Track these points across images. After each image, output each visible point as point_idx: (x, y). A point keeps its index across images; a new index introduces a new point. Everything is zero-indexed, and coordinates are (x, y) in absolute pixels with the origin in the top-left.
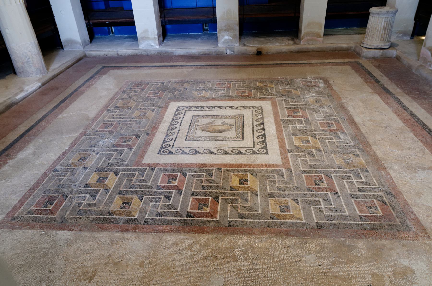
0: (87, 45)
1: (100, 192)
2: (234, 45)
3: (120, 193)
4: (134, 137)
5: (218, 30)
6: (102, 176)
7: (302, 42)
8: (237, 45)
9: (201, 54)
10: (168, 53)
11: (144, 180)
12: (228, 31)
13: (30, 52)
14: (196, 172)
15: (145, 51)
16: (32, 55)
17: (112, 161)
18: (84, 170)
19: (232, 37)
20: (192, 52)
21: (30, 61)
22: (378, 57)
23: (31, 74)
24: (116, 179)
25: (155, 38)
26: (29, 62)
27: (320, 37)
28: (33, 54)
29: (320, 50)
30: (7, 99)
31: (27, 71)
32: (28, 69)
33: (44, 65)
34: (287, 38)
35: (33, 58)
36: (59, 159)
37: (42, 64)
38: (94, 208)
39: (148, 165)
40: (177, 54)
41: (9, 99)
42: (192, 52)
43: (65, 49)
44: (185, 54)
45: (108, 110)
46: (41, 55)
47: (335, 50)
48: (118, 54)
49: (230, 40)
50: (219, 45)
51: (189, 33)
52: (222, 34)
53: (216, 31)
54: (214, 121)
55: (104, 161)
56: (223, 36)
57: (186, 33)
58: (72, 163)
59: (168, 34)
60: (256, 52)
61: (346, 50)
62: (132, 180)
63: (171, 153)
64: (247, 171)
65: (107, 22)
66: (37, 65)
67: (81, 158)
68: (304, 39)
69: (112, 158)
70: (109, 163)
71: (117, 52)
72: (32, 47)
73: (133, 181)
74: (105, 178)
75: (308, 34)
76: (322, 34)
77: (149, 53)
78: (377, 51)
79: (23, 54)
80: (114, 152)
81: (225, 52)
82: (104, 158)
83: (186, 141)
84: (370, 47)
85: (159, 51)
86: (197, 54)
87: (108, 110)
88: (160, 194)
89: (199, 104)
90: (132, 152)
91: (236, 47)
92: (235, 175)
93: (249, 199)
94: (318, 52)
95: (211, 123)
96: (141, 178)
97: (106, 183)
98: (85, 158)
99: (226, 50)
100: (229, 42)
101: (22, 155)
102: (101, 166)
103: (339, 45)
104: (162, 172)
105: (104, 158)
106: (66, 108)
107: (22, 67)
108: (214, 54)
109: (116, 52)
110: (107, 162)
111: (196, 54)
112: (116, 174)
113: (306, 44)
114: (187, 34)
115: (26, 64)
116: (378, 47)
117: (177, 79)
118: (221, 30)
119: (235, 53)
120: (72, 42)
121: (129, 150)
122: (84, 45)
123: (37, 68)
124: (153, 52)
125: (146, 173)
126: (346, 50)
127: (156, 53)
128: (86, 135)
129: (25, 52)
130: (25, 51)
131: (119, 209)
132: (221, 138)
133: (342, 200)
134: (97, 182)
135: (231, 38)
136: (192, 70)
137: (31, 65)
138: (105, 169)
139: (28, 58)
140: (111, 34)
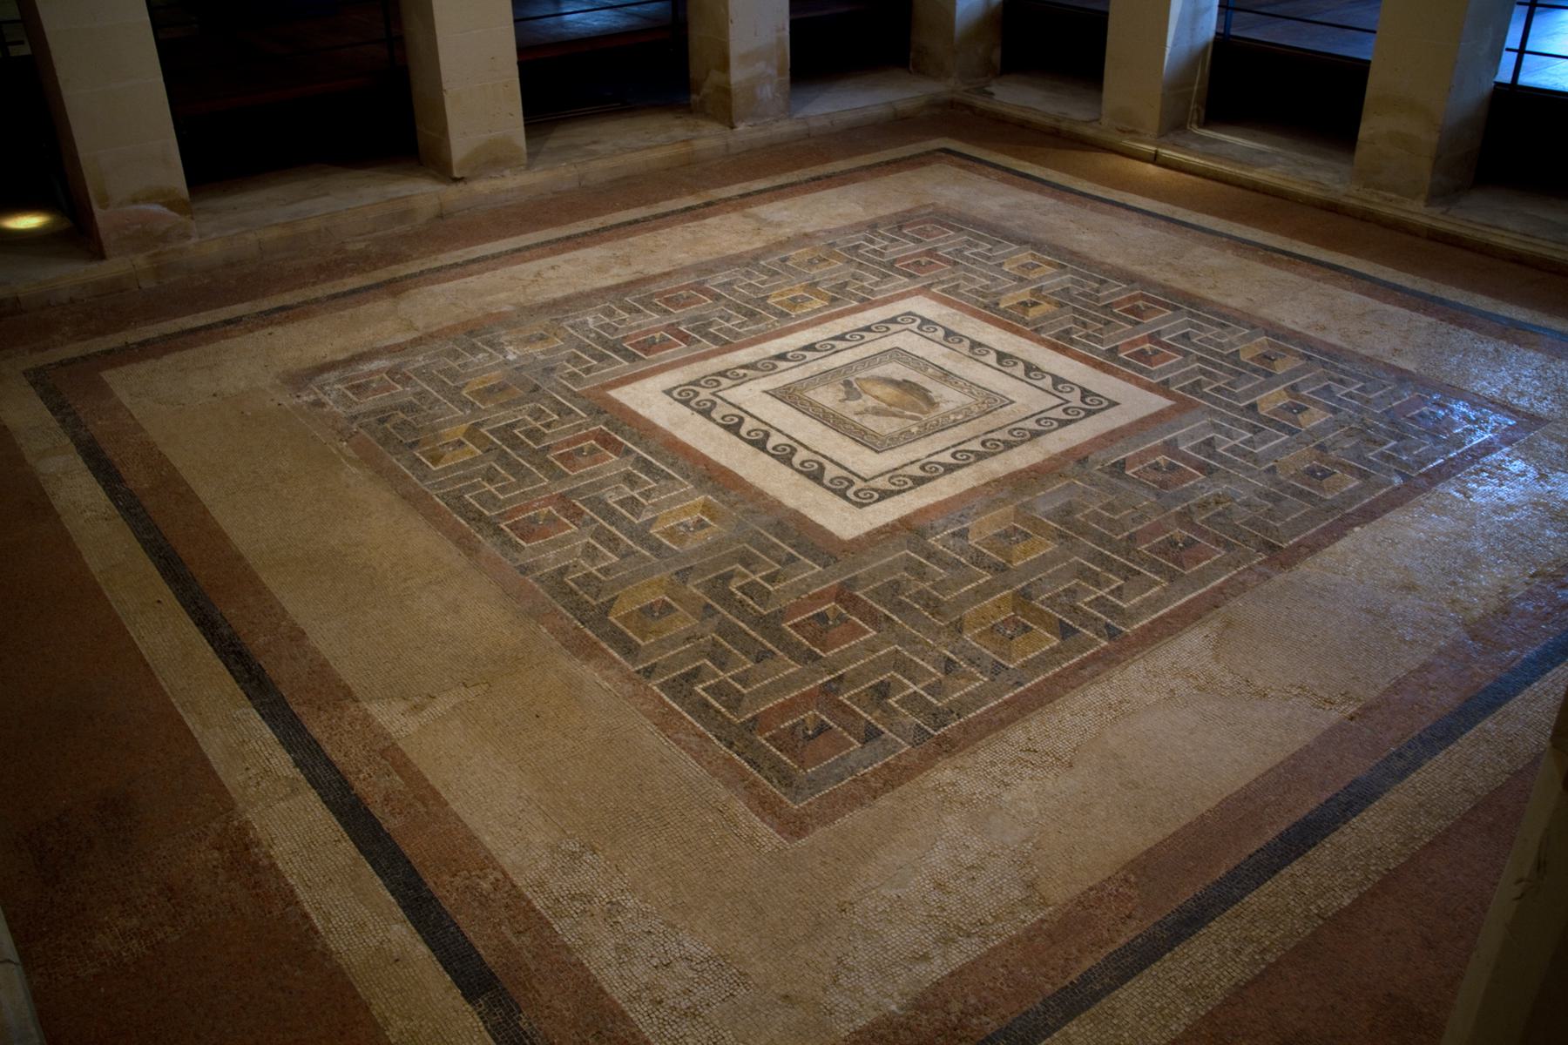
3: (1269, 375)
4: (1129, 473)
6: (1288, 414)
11: (1204, 374)
14: (1084, 344)
17: (1243, 435)
18: (1327, 444)
24: (1262, 400)
39: (1167, 394)
45: (1112, 633)
55: (1264, 442)
62: (1228, 384)
63: (1085, 393)
67: (1322, 478)
69: (1237, 442)
70: (1255, 433)
73: (1226, 381)
74: (1288, 408)
80: (1221, 455)
82: (1260, 450)
83: (1014, 399)
87: (1112, 633)
88: (1194, 345)
90: (1175, 434)
96: (1204, 378)
97: (1287, 400)
98: (1311, 472)
102: (1278, 437)
104: (1152, 371)
105: (1260, 450)
110: (1256, 438)
112: (1253, 407)
121: (1179, 442)
125: (1186, 383)
128: (1272, 547)
134: (1307, 408)
138: (1272, 424)
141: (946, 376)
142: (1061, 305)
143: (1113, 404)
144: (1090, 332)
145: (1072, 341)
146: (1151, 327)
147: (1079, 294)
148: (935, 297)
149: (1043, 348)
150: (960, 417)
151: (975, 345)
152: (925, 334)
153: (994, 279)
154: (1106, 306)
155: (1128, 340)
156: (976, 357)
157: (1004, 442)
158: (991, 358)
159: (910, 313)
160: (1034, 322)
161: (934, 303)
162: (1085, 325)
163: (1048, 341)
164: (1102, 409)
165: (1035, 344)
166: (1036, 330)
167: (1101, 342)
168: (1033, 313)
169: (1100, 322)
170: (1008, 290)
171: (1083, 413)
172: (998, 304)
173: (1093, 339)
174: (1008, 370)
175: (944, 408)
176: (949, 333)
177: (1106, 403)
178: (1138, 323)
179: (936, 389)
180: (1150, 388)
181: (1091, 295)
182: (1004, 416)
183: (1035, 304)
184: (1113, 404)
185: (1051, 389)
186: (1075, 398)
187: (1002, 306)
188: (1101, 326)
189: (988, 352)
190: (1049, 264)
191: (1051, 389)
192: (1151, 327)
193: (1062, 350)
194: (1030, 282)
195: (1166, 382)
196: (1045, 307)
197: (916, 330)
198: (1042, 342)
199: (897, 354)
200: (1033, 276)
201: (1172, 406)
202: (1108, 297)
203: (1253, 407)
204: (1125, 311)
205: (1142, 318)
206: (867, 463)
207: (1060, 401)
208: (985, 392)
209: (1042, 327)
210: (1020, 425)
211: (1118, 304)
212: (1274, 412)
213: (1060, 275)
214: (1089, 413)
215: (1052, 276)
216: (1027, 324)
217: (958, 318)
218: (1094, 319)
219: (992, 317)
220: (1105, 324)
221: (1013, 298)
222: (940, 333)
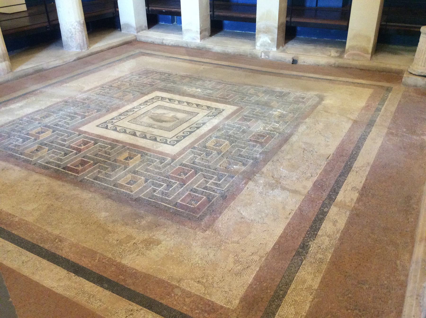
0: (142, 30)
1: (31, 140)
2: (272, 50)
5: (256, 31)
7: (345, 56)
8: (275, 49)
9: (237, 54)
10: (206, 48)
12: (266, 33)
13: (74, 29)
14: (106, 144)
15: (187, 43)
16: (75, 31)
19: (271, 41)
20: (228, 51)
21: (73, 37)
22: (421, 86)
23: (72, 48)
25: (197, 31)
26: (72, 37)
27: (368, 53)
28: (77, 31)
29: (364, 68)
30: (39, 65)
31: (69, 45)
32: (71, 44)
33: (85, 42)
34: (336, 49)
35: (76, 34)
36: (31, 114)
37: (83, 41)
38: (16, 148)
40: (214, 51)
41: (41, 65)
42: (228, 51)
43: (122, 31)
44: (222, 52)
46: (85, 33)
47: (382, 71)
48: (162, 43)
49: (268, 43)
50: (256, 47)
51: (245, 31)
52: (260, 36)
53: (255, 31)
54: (169, 113)
56: (260, 37)
57: (242, 31)
58: (36, 118)
59: (225, 30)
60: (291, 61)
61: (396, 73)
63: (107, 128)
64: (139, 152)
65: (164, 10)
66: (78, 41)
68: (348, 53)
71: (163, 40)
72: (77, 25)
75: (353, 48)
76: (370, 50)
77: (189, 45)
78: (419, 78)
79: (68, 30)
81: (260, 55)
84: (413, 73)
85: (198, 46)
86: (232, 53)
89: (177, 97)
91: (273, 52)
92: (128, 152)
93: (116, 170)
94: (362, 70)
95: (164, 114)
97: (40, 135)
99: (261, 54)
100: (266, 46)
101: (12, 106)
103: (388, 66)
106: (76, 79)
107: (66, 41)
108: (249, 56)
109: (161, 41)
111: (232, 53)
113: (349, 59)
114: (243, 32)
115: (69, 39)
116: (422, 74)
117: (185, 74)
118: (260, 32)
119: (270, 58)
120: (128, 26)
122: (139, 29)
123: (78, 44)
124: (193, 46)
126: (396, 73)
127: (196, 47)
129: (70, 29)
130: (71, 27)
131: (29, 153)
132: (156, 126)
133: (180, 190)
135: (270, 42)
136: (209, 67)
137: (73, 40)
139: (72, 33)
140: (175, 23)
141: (151, 126)
142: (115, 161)
143: (97, 126)
144: (104, 150)
145: (110, 144)
146: (78, 157)
147: (107, 168)
148: (167, 155)
149: (121, 140)
150: (142, 116)
151: (145, 137)
152: (163, 138)
153: (147, 170)
154: (96, 164)
155: (89, 149)
156: (143, 133)
157: (128, 112)
158: (138, 134)
159: (173, 145)
160: (125, 150)
161: (167, 152)
162: (106, 153)
163: (119, 143)
164: (101, 124)
165: (124, 141)
166: (124, 147)
167: (100, 146)
168: (126, 155)
169: (100, 155)
170: (139, 165)
171: (107, 122)
172: (141, 156)
173: (102, 146)
174: (131, 130)
175: (147, 117)
176: (155, 140)
177: (100, 126)
178: (83, 157)
179: (151, 121)
180: (85, 132)
181: (102, 169)
182: (129, 118)
183: (126, 159)
184: (97, 126)
185: (117, 127)
186: (110, 125)
187: (139, 155)
188: (99, 153)
189: (140, 135)
190: (122, 186)
191: (117, 127)
192: (78, 157)
193: (114, 140)
194: (130, 171)
195: (79, 135)
196: (122, 158)
197: (167, 139)
198: (122, 142)
199: (169, 130)
200: (129, 176)
201: (79, 128)
202: (94, 169)
203: (53, 132)
204: (88, 162)
205: (82, 160)
206: (160, 103)
207: (114, 124)
208: (137, 123)
209: (122, 148)
210: (125, 116)
211: (90, 166)
212: (48, 130)
213: (116, 180)
214: (105, 122)
215: (120, 178)
216: (128, 148)
217: (155, 147)
218: (101, 156)
219: (142, 149)
220: (97, 154)
221: (136, 160)
222: (158, 139)
